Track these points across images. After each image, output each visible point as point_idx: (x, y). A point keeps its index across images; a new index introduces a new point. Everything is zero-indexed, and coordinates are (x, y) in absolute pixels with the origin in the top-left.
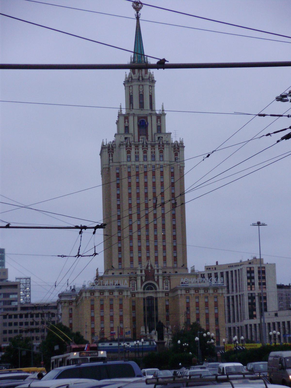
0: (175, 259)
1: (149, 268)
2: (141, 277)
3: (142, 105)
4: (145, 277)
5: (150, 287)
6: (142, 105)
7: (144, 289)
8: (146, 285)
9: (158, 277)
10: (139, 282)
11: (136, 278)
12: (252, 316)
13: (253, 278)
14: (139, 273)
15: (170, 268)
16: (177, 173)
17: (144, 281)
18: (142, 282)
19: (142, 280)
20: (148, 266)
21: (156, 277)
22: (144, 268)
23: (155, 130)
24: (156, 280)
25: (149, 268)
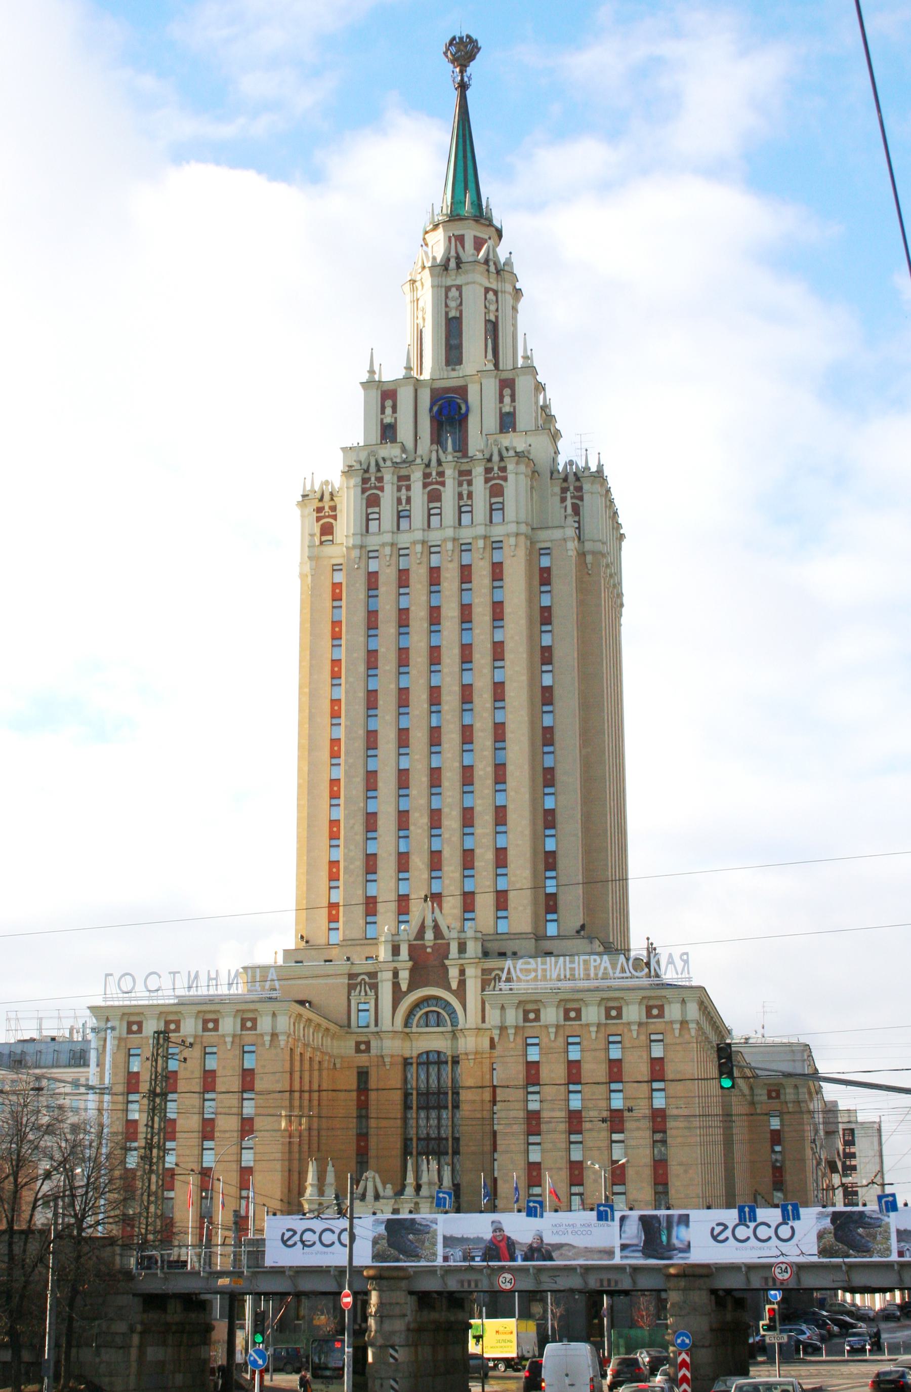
1: (429, 935)
2: (396, 974)
4: (412, 971)
5: (433, 1013)
7: (407, 1024)
8: (417, 1005)
9: (462, 972)
11: (373, 975)
17: (404, 987)
18: (398, 996)
19: (396, 985)
20: (422, 929)
21: (453, 973)
24: (454, 985)
25: (429, 935)
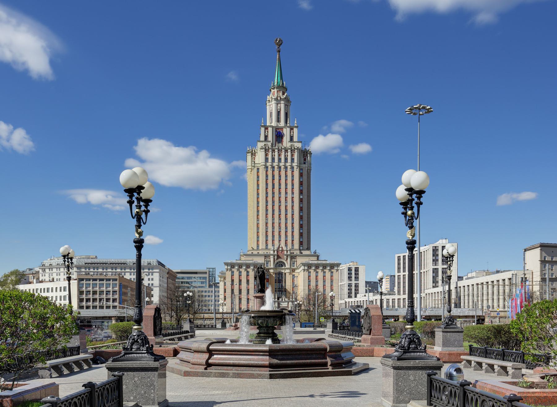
0: (301, 243)
1: (281, 249)
3: (278, 120)
6: (278, 120)
8: (277, 263)
10: (272, 260)
12: (350, 297)
13: (351, 274)
14: (272, 252)
15: (296, 250)
16: (305, 174)
19: (274, 259)
20: (279, 247)
22: (276, 249)
23: (289, 139)
